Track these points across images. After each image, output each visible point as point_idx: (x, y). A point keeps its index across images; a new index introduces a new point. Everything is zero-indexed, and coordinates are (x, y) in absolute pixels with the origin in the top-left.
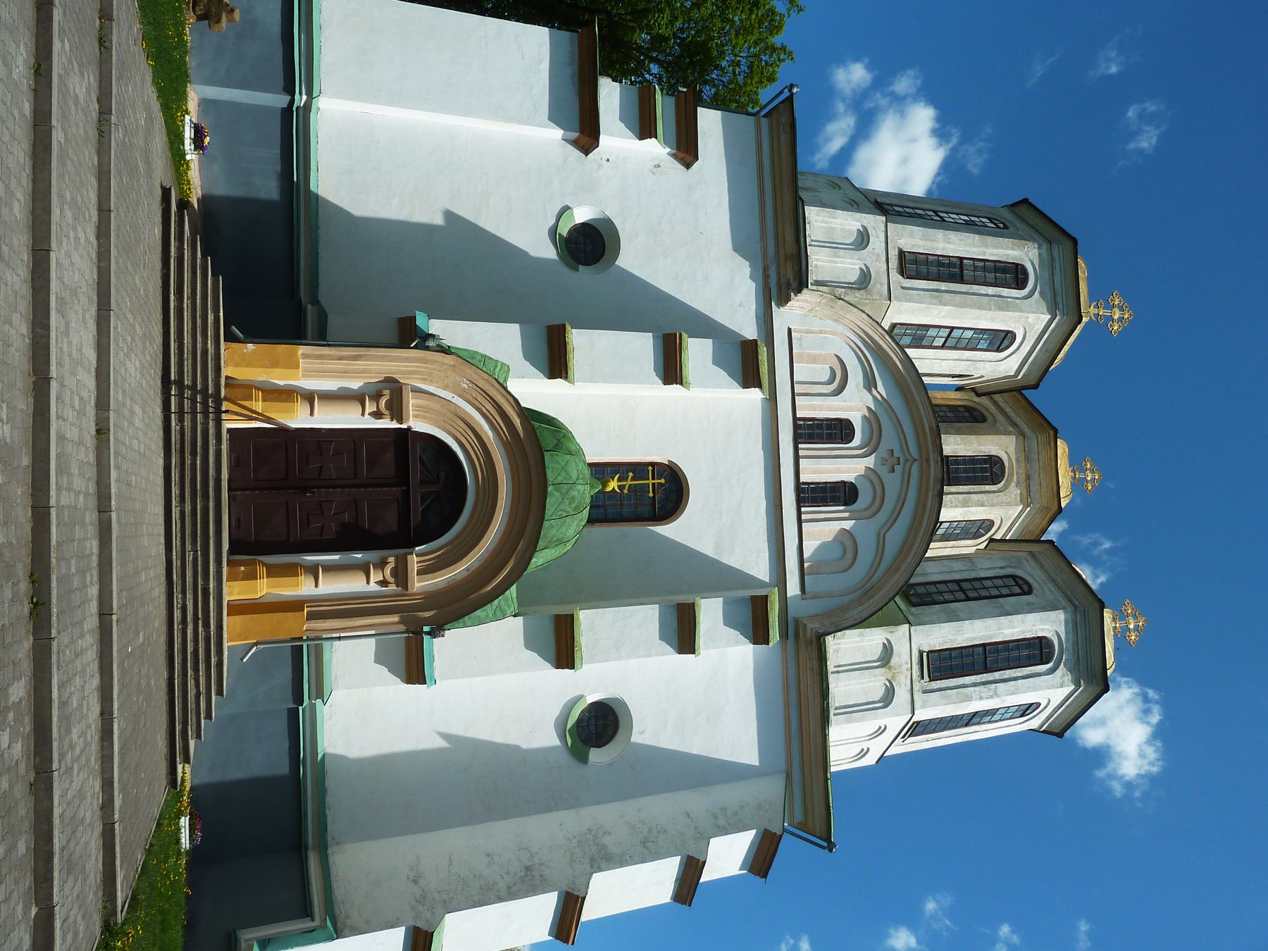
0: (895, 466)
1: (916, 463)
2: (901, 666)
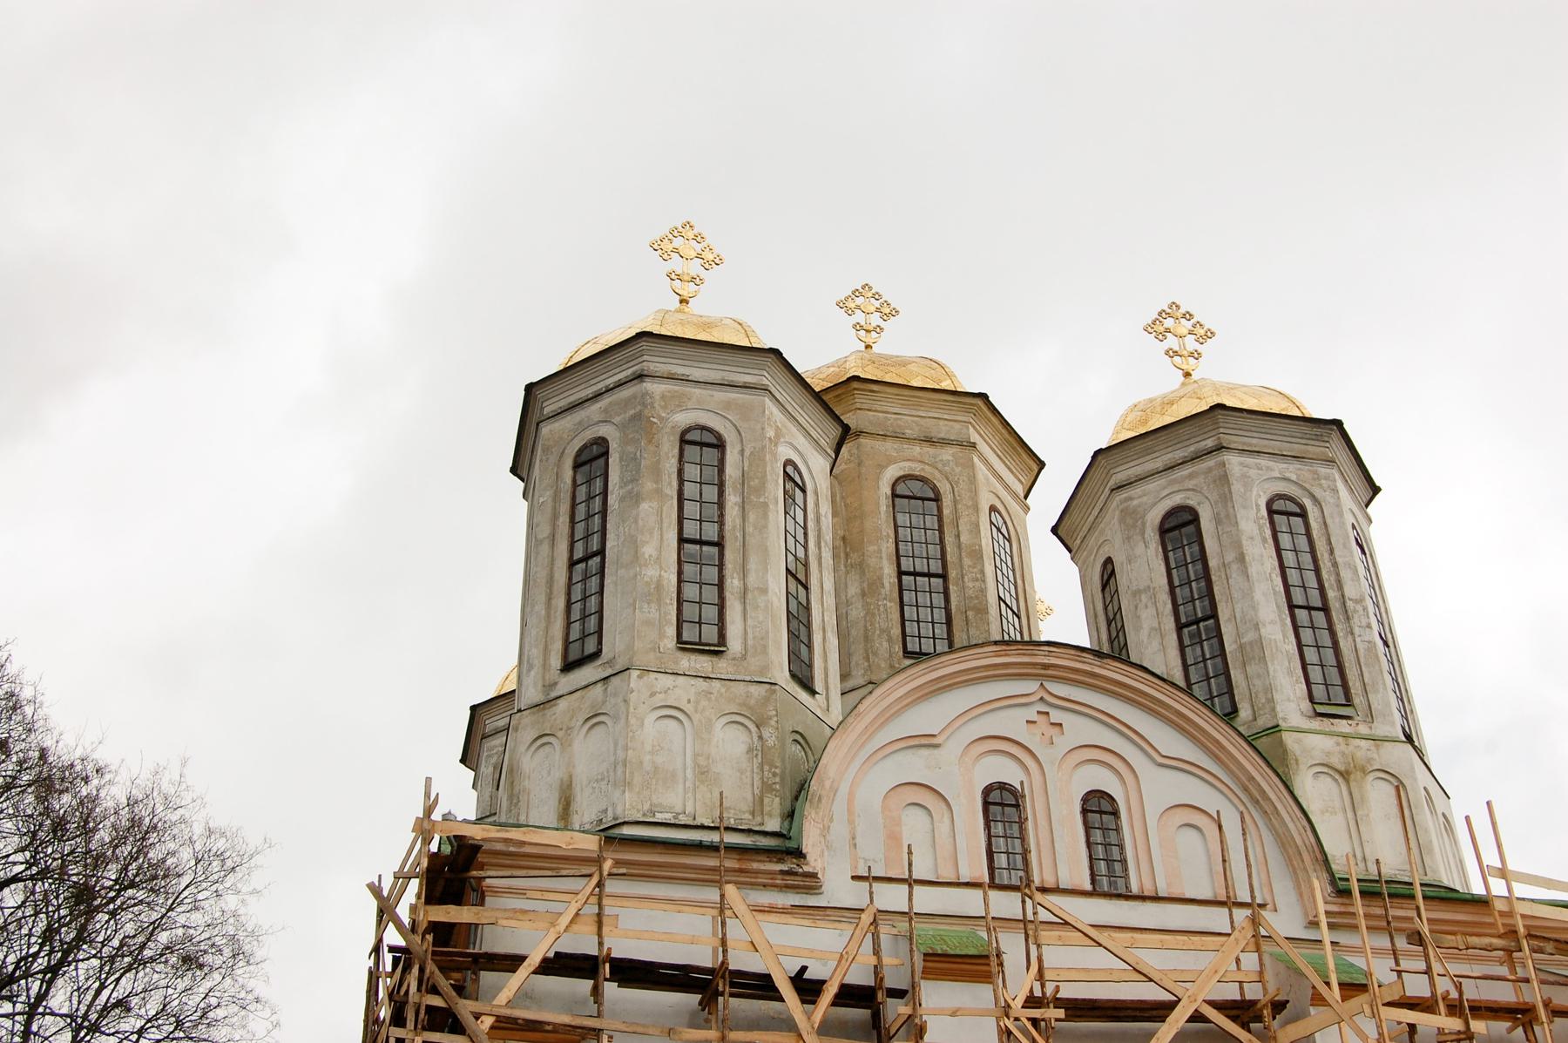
0: (1052, 721)
2: (1343, 754)
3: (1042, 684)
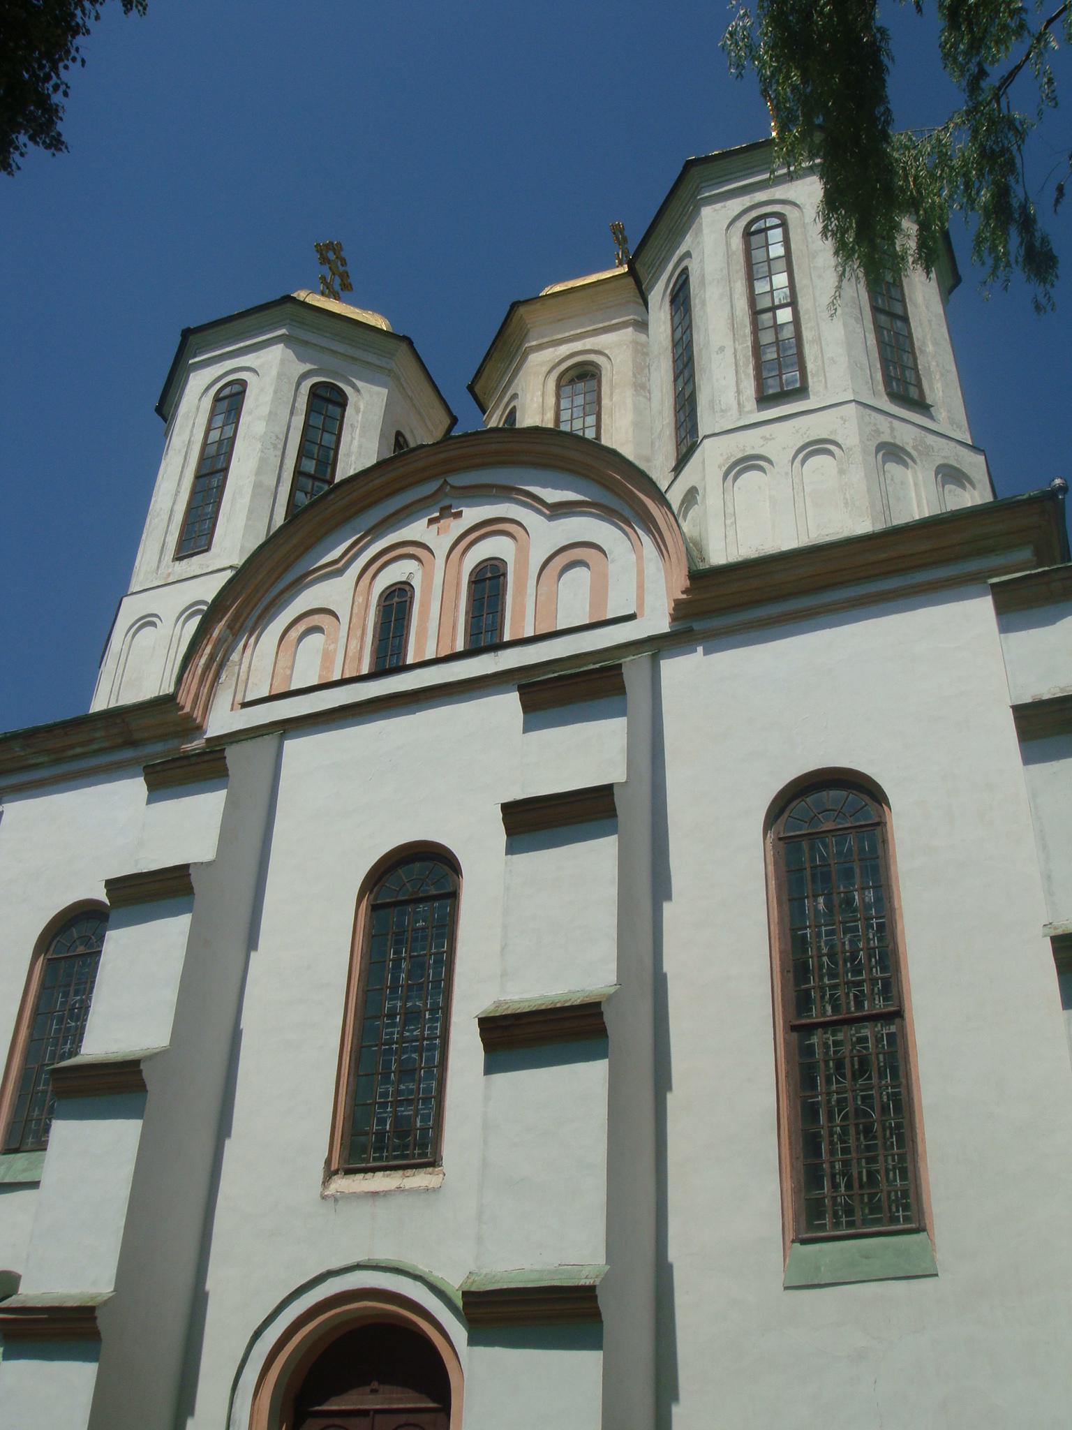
1: (447, 479)
3: (445, 480)
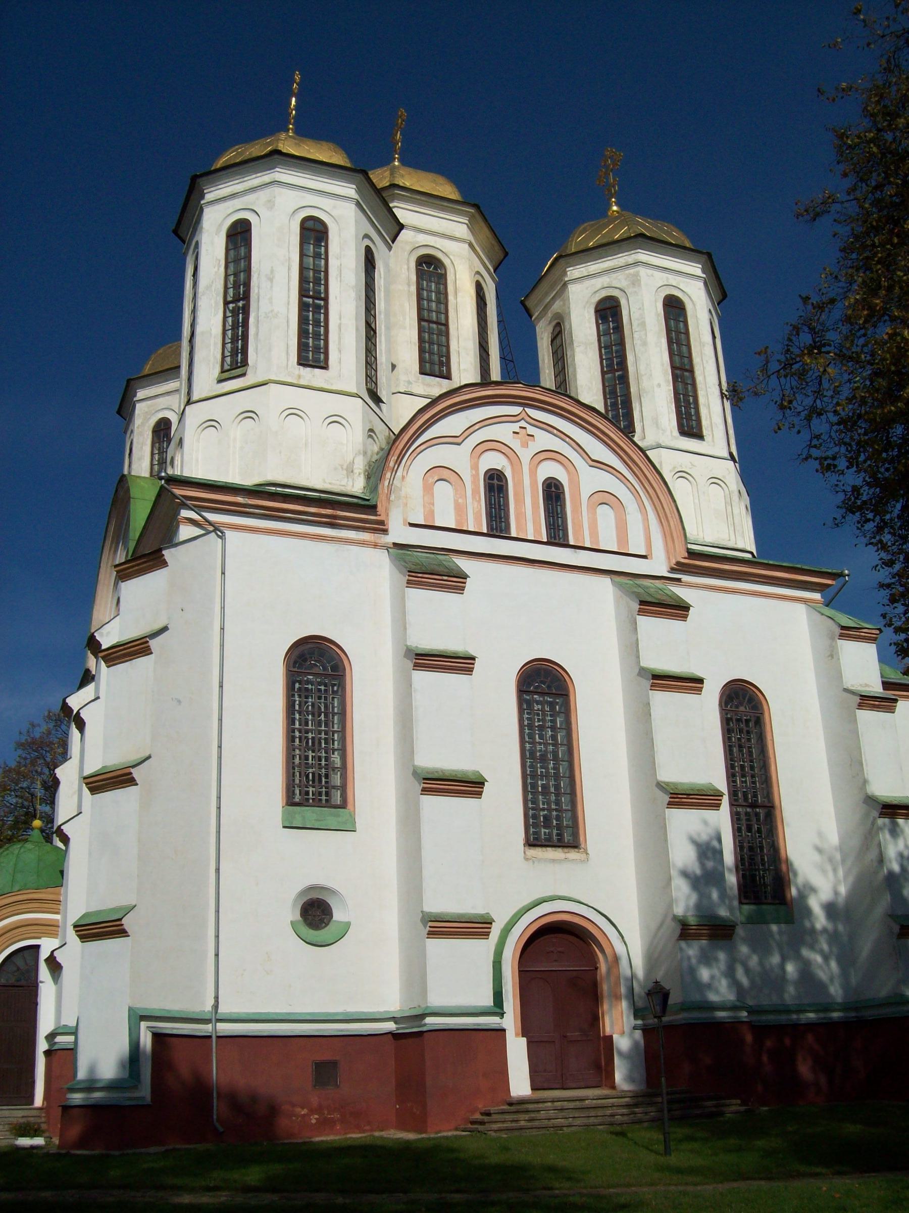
1: (525, 409)
3: (524, 409)
